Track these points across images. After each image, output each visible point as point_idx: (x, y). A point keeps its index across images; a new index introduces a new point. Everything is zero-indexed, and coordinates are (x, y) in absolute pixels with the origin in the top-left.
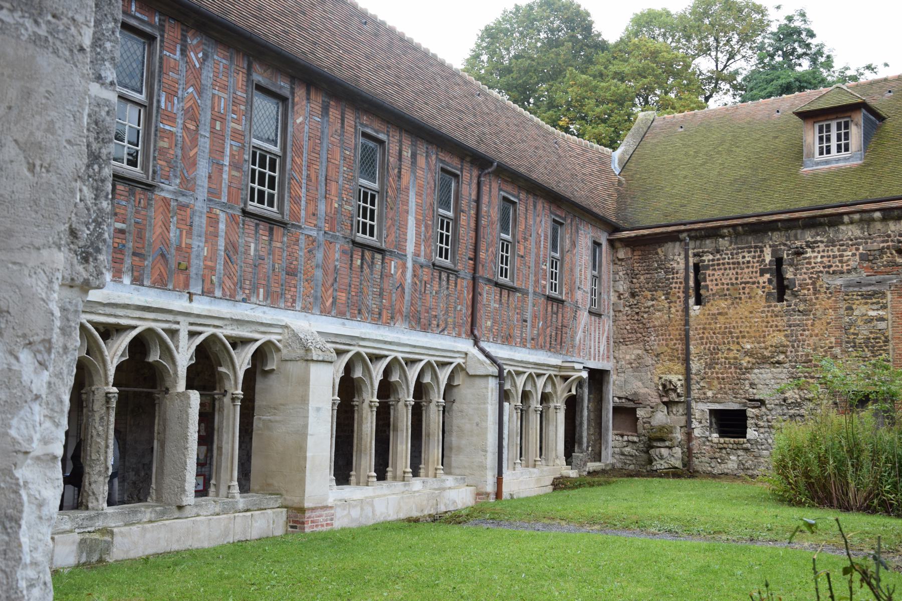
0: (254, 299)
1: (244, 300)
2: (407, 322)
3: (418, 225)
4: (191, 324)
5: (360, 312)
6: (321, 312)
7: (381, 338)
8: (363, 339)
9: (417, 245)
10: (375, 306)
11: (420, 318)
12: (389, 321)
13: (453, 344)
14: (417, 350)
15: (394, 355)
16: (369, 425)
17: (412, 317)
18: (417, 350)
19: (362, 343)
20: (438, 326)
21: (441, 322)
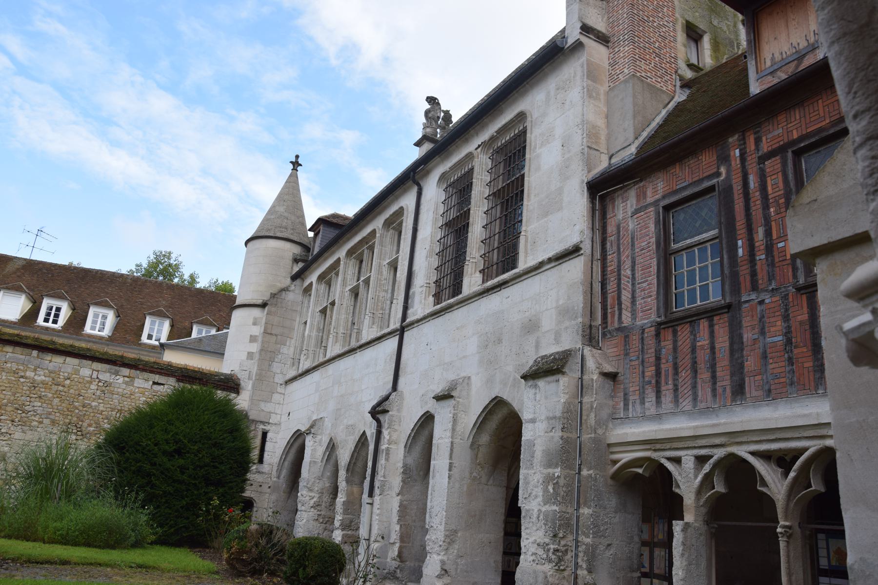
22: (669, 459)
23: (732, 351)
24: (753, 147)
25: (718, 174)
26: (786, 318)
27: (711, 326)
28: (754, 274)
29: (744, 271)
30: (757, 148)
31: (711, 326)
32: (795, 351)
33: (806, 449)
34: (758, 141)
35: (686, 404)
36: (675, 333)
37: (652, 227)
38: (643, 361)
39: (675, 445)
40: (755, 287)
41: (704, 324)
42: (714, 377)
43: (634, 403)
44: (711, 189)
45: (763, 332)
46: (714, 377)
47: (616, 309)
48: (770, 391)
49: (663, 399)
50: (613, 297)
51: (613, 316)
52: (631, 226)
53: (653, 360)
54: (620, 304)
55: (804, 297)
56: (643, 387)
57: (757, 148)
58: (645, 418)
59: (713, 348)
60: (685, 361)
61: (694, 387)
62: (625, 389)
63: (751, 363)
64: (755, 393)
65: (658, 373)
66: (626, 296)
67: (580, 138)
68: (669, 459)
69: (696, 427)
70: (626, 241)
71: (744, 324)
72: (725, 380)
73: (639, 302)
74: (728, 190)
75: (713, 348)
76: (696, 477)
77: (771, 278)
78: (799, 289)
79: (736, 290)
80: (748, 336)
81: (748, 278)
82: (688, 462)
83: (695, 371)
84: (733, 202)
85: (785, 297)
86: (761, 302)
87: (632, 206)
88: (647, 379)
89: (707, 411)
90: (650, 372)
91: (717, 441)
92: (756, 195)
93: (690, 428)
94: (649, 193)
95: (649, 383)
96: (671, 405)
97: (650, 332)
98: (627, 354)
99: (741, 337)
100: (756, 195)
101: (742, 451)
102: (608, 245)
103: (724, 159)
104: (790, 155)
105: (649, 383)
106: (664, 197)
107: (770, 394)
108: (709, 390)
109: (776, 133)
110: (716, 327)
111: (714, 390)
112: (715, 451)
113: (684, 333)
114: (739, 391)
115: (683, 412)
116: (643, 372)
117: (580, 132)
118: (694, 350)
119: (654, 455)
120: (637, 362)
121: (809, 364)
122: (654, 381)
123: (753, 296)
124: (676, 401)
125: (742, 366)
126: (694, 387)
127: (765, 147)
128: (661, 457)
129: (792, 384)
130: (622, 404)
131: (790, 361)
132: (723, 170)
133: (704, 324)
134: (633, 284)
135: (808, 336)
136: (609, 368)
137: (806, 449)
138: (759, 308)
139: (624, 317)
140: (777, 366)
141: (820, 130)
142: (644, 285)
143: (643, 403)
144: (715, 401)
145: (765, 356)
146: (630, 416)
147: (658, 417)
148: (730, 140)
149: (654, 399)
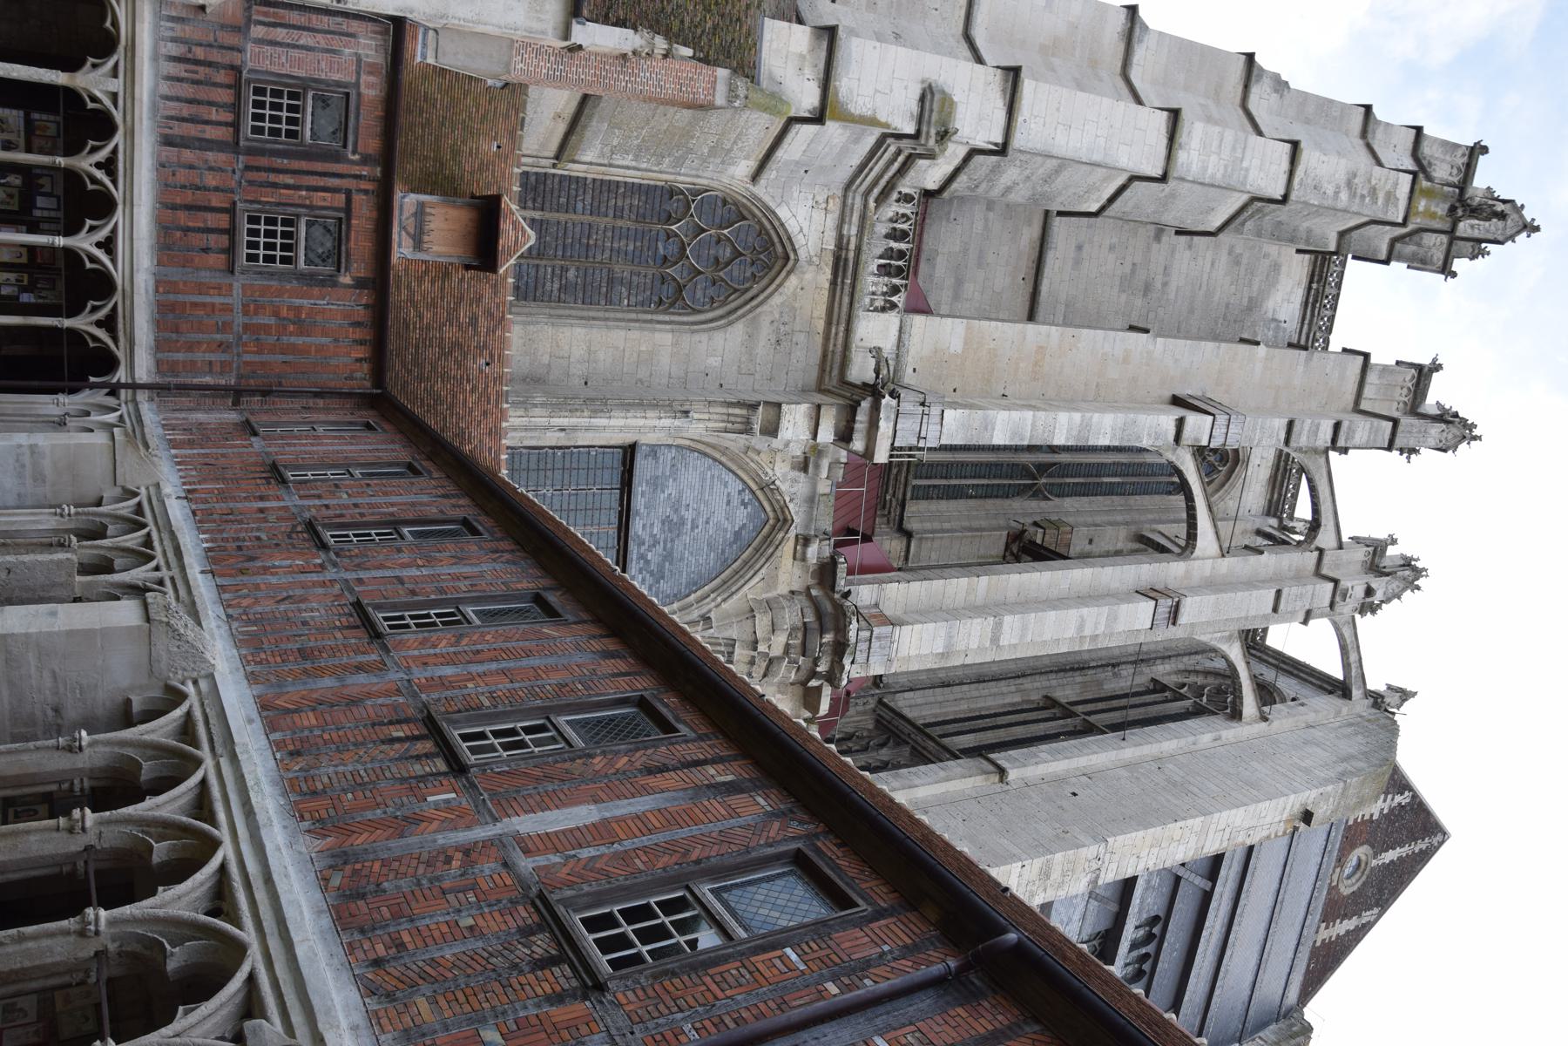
0: (235, 625)
1: (228, 616)
2: (330, 861)
3: (600, 832)
4: (172, 579)
5: (295, 754)
6: (259, 697)
7: (250, 783)
8: (234, 758)
9: (550, 842)
10: (326, 780)
11: (363, 896)
12: (307, 815)
13: (344, 1024)
14: (261, 895)
15: (248, 935)
16: (25, 757)
17: (355, 872)
18: (261, 895)
19: (224, 762)
20: (377, 963)
21: (394, 969)
22: (116, 66)
23: (201, 140)
24: (363, 187)
25: (354, 152)
26: (217, 189)
27: (226, 124)
28: (258, 169)
29: (263, 161)
30: (360, 191)
31: (226, 124)
32: (190, 192)
33: (117, 189)
34: (366, 192)
35: (165, 88)
36: (229, 87)
37: (336, 77)
38: (210, 46)
39: (129, 74)
40: (248, 168)
41: (229, 117)
42: (183, 120)
43: (172, 29)
44: (345, 146)
45: (211, 169)
46: (183, 120)
47: (272, 20)
48: (164, 167)
49: (172, 64)
50: (283, 17)
51: (266, 14)
52: (347, 51)
53: (210, 59)
54: (275, 25)
55: (227, 205)
56: (186, 43)
57: (360, 191)
58: (158, 40)
59: (207, 122)
60: (203, 93)
61: (178, 99)
62: (189, 19)
63: (188, 155)
64: (164, 154)
65: (197, 62)
66: (280, 34)
67: (462, 16)
68: (116, 66)
69: (141, 102)
70: (336, 42)
71: (220, 154)
72: (179, 129)
73: (268, 49)
74: (337, 157)
75: (207, 122)
76: (101, 91)
77: (251, 183)
78: (234, 203)
79: (250, 152)
80: (210, 155)
81: (256, 164)
82: (116, 85)
83: (190, 101)
84: (325, 161)
85: (232, 191)
86: (234, 172)
87: (367, 56)
88: (194, 48)
89: (154, 108)
90: (199, 53)
91: (129, 118)
92: (321, 182)
93: (141, 94)
94: (372, 79)
95: (190, 51)
96: (165, 73)
97: (236, 58)
98: (223, 27)
99: (211, 150)
100: (321, 182)
101: (118, 138)
102: (339, 19)
103: (365, 160)
104: (342, 215)
105: (190, 51)
106: (359, 94)
107: (161, 165)
108: (173, 113)
109: (364, 208)
110: (224, 128)
111: (172, 118)
112: (121, 114)
113: (225, 96)
114: (167, 141)
115: (157, 85)
116: (201, 45)
117: (469, 16)
118: (210, 104)
119: (121, 48)
120: (212, 39)
121: (178, 200)
122: (190, 56)
123: (241, 166)
124: (169, 78)
125: (187, 147)
126: (178, 99)
127: (358, 198)
128: (119, 55)
129: (166, 185)
130: (174, 14)
131: (183, 187)
132: (357, 157)
133: (229, 117)
134: (288, 45)
135: (199, 203)
136: (208, 10)
137: (117, 189)
138: (230, 169)
139: (260, 28)
140: (183, 176)
141: (348, 239)
142: (283, 59)
143: (174, 40)
144: (162, 117)
145: (191, 167)
146: (162, 23)
147: (155, 58)
148: (379, 169)
149: (174, 53)
